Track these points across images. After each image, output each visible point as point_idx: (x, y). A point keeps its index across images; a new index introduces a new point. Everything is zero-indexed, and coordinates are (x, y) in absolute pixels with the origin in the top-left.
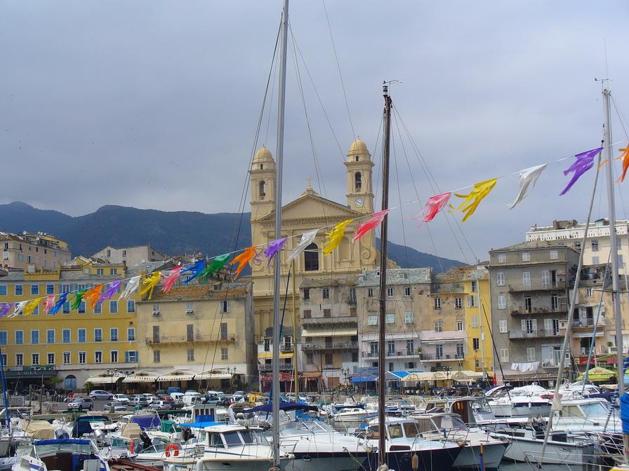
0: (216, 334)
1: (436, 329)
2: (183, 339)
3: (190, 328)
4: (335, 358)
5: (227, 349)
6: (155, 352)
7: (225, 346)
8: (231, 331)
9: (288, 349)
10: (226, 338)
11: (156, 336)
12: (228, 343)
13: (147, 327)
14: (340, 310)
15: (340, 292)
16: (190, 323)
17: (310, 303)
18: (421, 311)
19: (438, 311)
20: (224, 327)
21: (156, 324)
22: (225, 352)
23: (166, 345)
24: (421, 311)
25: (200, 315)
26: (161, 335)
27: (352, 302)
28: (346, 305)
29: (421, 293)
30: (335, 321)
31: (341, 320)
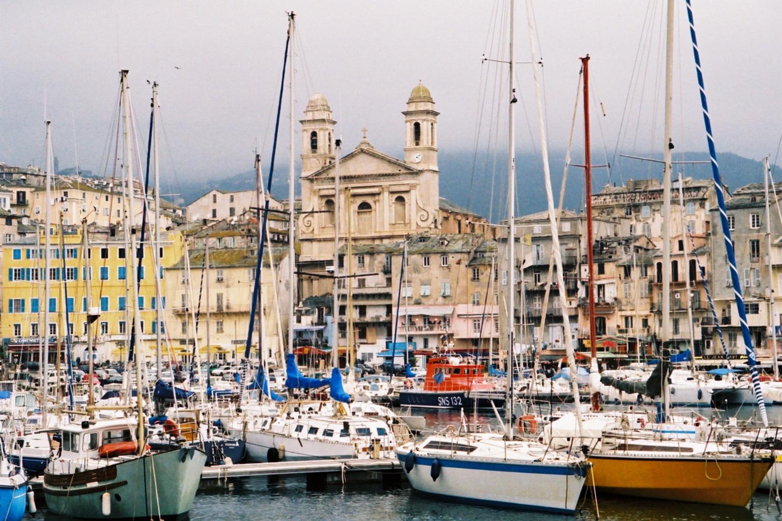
1: (474, 303)
4: (369, 333)
9: (321, 321)
22: (220, 324)
24: (457, 283)
25: (230, 283)
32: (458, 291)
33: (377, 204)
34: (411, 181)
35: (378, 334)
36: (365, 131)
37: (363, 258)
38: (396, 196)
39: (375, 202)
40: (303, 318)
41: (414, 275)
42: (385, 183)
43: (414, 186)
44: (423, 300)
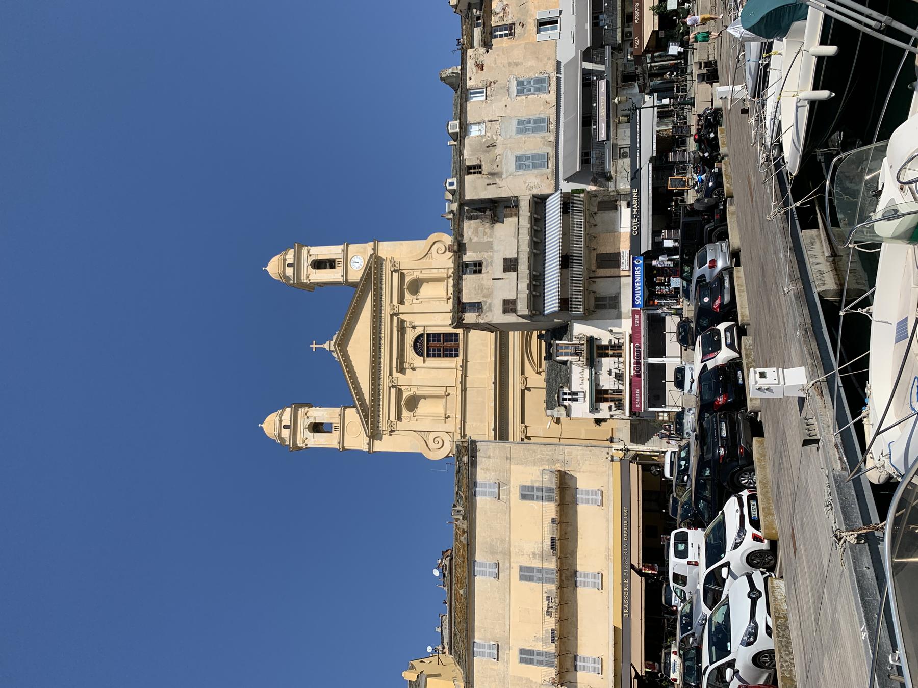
13: (521, 679)
14: (507, 238)
15: (471, 240)
16: (515, 574)
17: (489, 301)
18: (517, 64)
19: (518, 30)
21: (515, 655)
24: (517, 64)
28: (498, 226)
29: (481, 67)
30: (525, 249)
31: (525, 238)
33: (416, 324)
34: (387, 268)
35: (613, 229)
38: (407, 295)
39: (414, 327)
42: (386, 312)
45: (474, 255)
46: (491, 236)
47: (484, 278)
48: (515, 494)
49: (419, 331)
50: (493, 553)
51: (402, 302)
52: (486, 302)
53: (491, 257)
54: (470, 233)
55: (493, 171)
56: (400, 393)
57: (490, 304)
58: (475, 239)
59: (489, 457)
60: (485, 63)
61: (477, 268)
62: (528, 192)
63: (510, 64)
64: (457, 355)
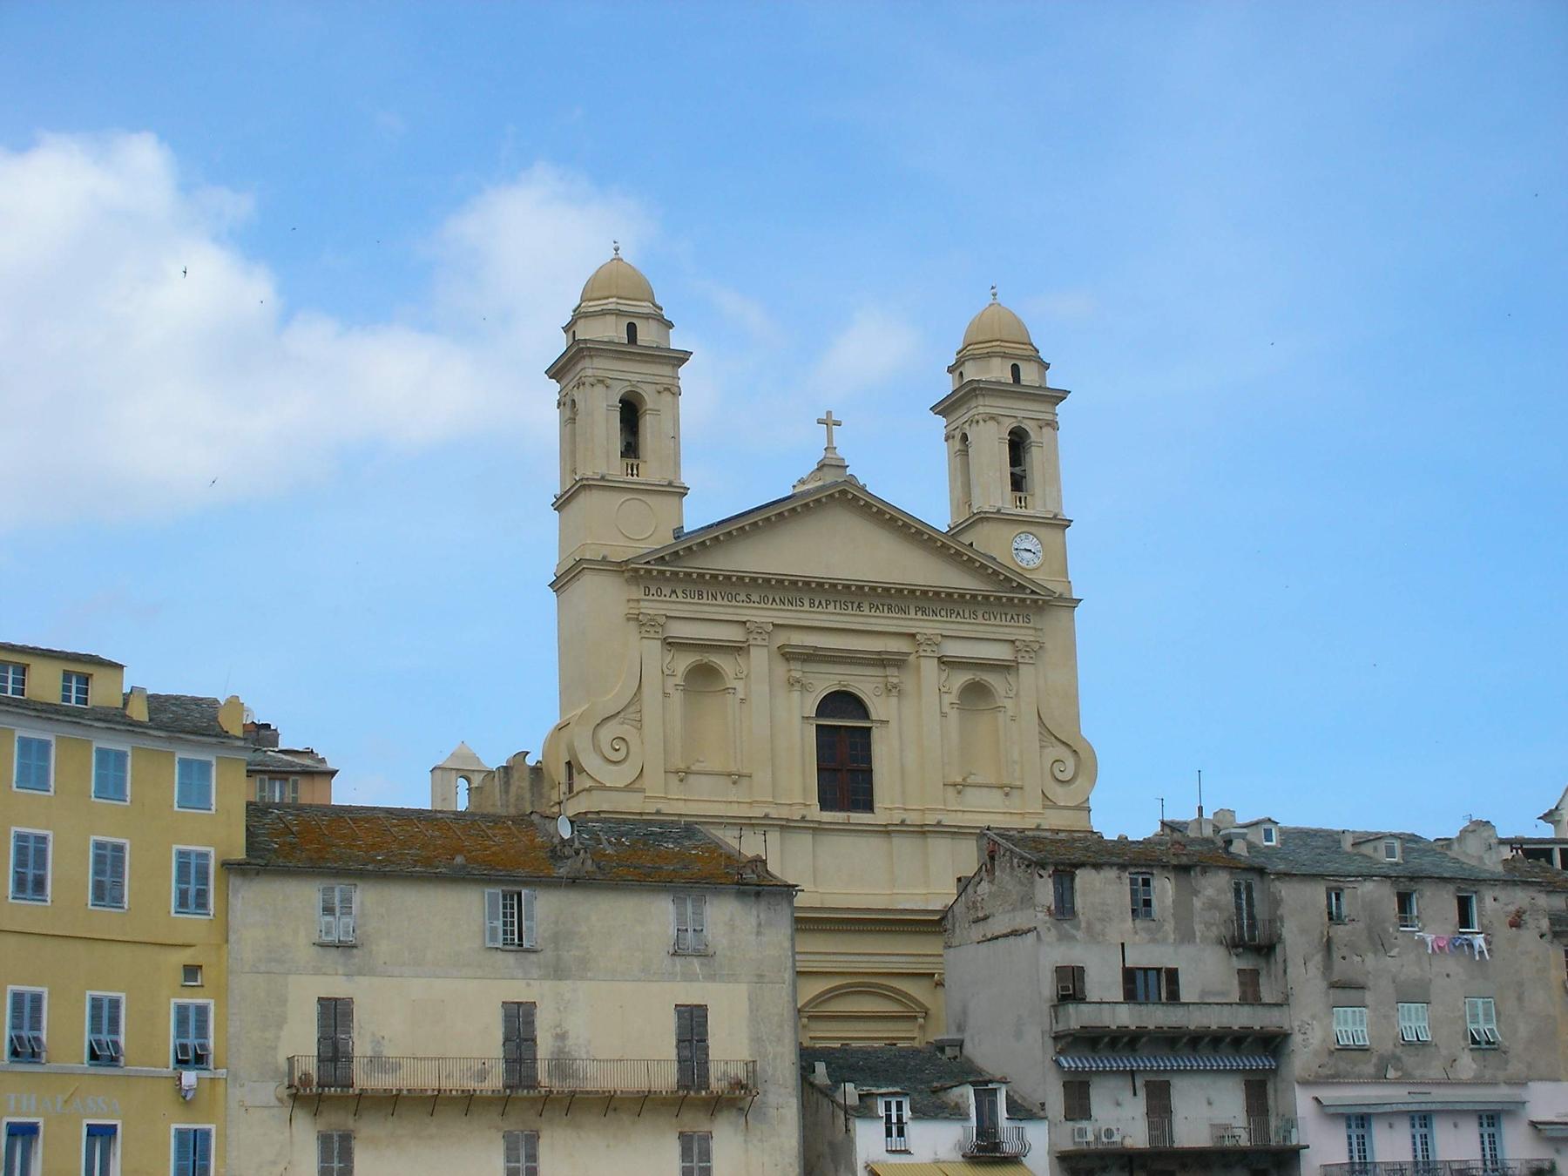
0: (653, 1058)
2: (482, 1075)
3: (519, 1024)
5: (708, 1137)
6: (325, 1140)
7: (695, 1122)
8: (728, 1050)
10: (704, 1083)
11: (334, 1051)
12: (716, 1105)
15: (1196, 893)
16: (519, 991)
17: (1079, 935)
18: (1520, 998)
20: (692, 1024)
21: (337, 987)
23: (393, 1103)
24: (1520, 998)
26: (361, 1047)
27: (1255, 945)
28: (1221, 952)
29: (1516, 922)
32: (1523, 1030)
34: (1023, 634)
36: (829, 422)
37: (1146, 883)
38: (961, 679)
40: (915, 1130)
41: (1370, 959)
42: (927, 626)
43: (1034, 650)
44: (1409, 1061)
45: (1169, 901)
46: (1204, 939)
47: (1124, 926)
48: (692, 994)
49: (879, 707)
50: (556, 939)
51: (945, 662)
52: (1078, 928)
53: (1164, 940)
54: (1210, 892)
55: (1334, 948)
56: (737, 649)
57: (1073, 938)
58: (1197, 903)
59: (758, 933)
60: (1522, 932)
61: (1142, 907)
62: (1296, 1024)
63: (1521, 984)
64: (825, 805)
